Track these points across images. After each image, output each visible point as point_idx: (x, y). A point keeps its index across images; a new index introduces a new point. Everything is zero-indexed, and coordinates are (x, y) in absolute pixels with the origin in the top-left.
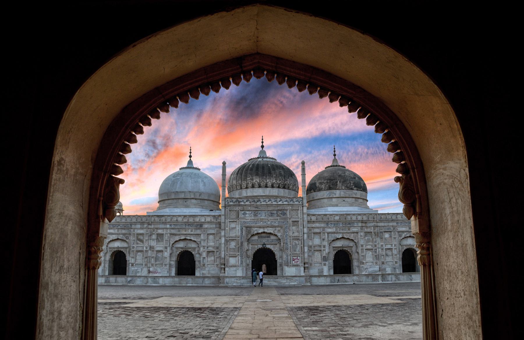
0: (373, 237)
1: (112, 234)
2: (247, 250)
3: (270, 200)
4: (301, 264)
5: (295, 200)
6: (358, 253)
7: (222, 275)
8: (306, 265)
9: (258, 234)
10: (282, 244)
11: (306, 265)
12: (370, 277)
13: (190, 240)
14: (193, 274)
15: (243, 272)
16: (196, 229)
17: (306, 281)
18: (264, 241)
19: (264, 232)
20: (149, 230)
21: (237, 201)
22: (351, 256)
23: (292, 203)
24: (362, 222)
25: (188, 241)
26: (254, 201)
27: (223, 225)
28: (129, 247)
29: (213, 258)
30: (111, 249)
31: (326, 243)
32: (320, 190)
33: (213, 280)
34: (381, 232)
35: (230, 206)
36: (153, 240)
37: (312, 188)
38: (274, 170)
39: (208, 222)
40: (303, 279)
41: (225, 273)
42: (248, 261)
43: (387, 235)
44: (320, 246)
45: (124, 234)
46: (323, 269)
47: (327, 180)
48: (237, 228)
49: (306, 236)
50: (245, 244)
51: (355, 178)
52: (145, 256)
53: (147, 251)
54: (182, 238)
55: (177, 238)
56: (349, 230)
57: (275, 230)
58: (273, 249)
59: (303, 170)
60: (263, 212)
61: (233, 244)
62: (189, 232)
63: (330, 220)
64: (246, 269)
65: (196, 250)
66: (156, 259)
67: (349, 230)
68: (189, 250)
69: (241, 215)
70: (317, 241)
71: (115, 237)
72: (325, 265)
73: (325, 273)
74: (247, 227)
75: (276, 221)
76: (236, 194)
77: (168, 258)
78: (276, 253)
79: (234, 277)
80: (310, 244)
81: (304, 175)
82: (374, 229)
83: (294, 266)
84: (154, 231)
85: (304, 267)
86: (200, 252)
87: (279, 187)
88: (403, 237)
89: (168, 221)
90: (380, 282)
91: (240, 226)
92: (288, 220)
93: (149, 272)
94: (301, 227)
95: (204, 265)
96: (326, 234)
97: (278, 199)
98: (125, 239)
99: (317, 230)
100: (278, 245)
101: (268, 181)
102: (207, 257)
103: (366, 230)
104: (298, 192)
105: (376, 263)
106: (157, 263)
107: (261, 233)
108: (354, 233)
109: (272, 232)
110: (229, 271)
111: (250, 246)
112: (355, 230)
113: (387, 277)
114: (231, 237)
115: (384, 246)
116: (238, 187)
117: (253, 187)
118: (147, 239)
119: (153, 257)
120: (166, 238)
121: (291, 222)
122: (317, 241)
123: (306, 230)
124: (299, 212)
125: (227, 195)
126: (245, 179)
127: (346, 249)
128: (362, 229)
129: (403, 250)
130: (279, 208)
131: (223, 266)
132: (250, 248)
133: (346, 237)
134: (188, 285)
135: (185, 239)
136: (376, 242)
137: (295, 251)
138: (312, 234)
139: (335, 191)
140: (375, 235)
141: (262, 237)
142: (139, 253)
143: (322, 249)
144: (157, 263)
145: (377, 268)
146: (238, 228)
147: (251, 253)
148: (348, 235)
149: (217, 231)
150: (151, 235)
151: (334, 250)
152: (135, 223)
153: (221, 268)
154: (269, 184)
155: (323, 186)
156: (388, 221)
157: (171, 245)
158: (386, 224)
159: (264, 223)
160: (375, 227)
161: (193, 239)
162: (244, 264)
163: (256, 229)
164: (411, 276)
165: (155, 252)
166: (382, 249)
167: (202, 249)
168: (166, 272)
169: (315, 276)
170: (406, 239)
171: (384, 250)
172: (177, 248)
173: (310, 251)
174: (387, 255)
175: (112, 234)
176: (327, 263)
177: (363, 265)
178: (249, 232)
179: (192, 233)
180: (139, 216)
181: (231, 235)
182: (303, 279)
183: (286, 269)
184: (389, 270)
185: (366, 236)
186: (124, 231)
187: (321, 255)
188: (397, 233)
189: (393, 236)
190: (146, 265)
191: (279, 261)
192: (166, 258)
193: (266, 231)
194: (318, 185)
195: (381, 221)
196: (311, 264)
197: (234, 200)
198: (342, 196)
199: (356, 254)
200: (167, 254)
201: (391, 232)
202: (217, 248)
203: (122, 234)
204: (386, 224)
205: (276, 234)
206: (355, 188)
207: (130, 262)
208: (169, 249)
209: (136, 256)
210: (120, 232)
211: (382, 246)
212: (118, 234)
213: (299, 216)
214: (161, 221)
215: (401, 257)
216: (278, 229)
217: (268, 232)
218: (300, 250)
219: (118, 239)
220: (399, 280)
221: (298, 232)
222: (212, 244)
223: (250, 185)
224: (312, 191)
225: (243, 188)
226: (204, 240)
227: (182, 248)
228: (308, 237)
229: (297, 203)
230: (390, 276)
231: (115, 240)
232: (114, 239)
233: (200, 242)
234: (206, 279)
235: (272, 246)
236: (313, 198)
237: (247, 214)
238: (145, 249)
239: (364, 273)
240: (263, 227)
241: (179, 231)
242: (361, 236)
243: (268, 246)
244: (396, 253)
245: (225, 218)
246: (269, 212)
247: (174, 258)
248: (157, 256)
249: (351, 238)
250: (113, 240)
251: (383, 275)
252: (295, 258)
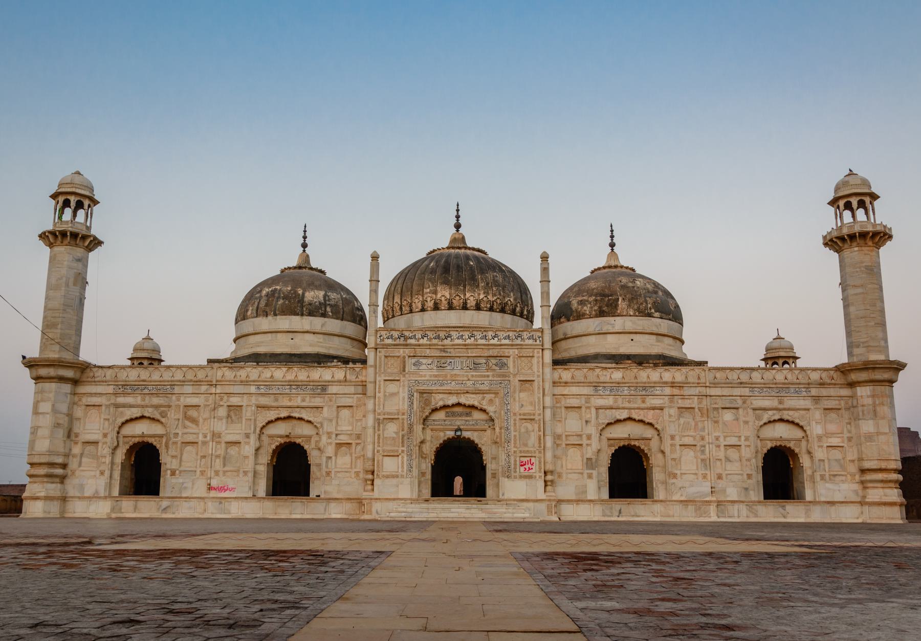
0: (698, 418)
1: (131, 406)
2: (422, 442)
3: (472, 336)
4: (538, 475)
5: (525, 335)
6: (663, 452)
7: (366, 495)
8: (549, 477)
9: (445, 407)
10: (497, 429)
11: (549, 477)
12: (691, 508)
13: (300, 419)
14: (307, 493)
15: (412, 491)
16: (314, 395)
17: (549, 512)
18: (459, 422)
19: (459, 404)
20: (211, 398)
21: (402, 336)
22: (648, 459)
23: (519, 341)
24: (673, 385)
25: (295, 422)
26: (438, 337)
27: (370, 387)
28: (166, 435)
29: (347, 459)
30: (126, 439)
31: (592, 430)
32: (580, 316)
33: (348, 506)
34: (716, 409)
35: (387, 346)
36: (220, 419)
37: (562, 313)
38: (482, 272)
39: (340, 381)
40: (543, 507)
41: (373, 490)
42: (424, 466)
43: (728, 416)
44: (580, 436)
45: (156, 407)
46: (586, 486)
47: (596, 295)
48: (401, 395)
49: (548, 413)
50: (418, 428)
51: (656, 293)
52: (200, 454)
53: (205, 443)
54: (282, 415)
55: (272, 415)
56: (643, 402)
57: (483, 398)
58: (476, 442)
59: (545, 270)
60: (457, 360)
61: (391, 429)
62: (298, 401)
63: (602, 379)
64: (420, 483)
65: (313, 441)
66: (225, 460)
67: (643, 402)
68: (298, 441)
69: (410, 367)
70: (573, 424)
71: (136, 412)
72: (590, 476)
73: (592, 494)
74: (422, 393)
75: (485, 378)
76: (400, 322)
77: (252, 458)
78: (483, 449)
79: (394, 499)
80: (559, 431)
81: (545, 280)
82: (700, 403)
83: (521, 477)
84: (222, 399)
85: (545, 481)
86: (321, 445)
87: (491, 309)
88: (765, 420)
89: (252, 378)
90: (714, 518)
91: (406, 389)
92: (511, 379)
93: (210, 488)
94: (538, 394)
95: (328, 474)
96: (593, 411)
97: (490, 334)
98: (158, 416)
99: (574, 402)
100: (489, 432)
101: (468, 295)
102: (336, 456)
103: (681, 403)
104: (532, 322)
105: (705, 476)
106: (226, 469)
107: (453, 406)
108: (654, 409)
109: (476, 404)
110: (382, 487)
111: (429, 433)
112: (657, 402)
113: (730, 507)
114: (389, 414)
115: (722, 439)
116: (406, 309)
117: (436, 307)
118: (206, 415)
119: (218, 456)
120: (249, 414)
121: (517, 384)
122: (573, 424)
123: (548, 401)
124: (535, 360)
125: (380, 324)
126: (421, 292)
127: (637, 443)
128: (671, 401)
129: (765, 451)
130: (491, 353)
131: (371, 476)
132: (428, 438)
133: (637, 418)
134: (294, 516)
135: (289, 418)
136: (703, 429)
137: (526, 445)
138: (563, 409)
139: (611, 319)
140: (702, 416)
141: (453, 414)
142: (189, 448)
143: (585, 441)
144: (226, 469)
145: (706, 488)
146: (404, 394)
147: (430, 449)
148: (642, 412)
149: (359, 400)
150: (214, 409)
151: (610, 446)
152: (183, 383)
153: (366, 480)
154: (472, 302)
155: (587, 309)
156: (729, 384)
157: (258, 429)
158: (726, 392)
159: (458, 380)
160: (701, 396)
161: (306, 418)
162: (415, 472)
163: (441, 396)
164: (783, 507)
165: (223, 445)
166: (719, 446)
167: (324, 439)
168: (247, 489)
169: (569, 501)
170: (771, 425)
171: (722, 448)
172: (270, 436)
173: (558, 445)
174: (728, 459)
175: (131, 406)
176: (595, 473)
177: (674, 481)
178: (427, 402)
179: (304, 404)
180: (190, 367)
181: (387, 409)
182: (543, 507)
183: (506, 483)
184: (732, 493)
185: (680, 416)
186: (156, 401)
187: (582, 456)
188: (750, 411)
189: (742, 419)
190: (202, 473)
191: (490, 467)
192: (246, 457)
193: (463, 400)
194: (575, 304)
195: (715, 385)
196: (560, 476)
197: (396, 334)
198: (627, 329)
199: (660, 455)
200: (248, 449)
201: (737, 408)
202: (358, 437)
203: (152, 406)
204: (726, 392)
205: (485, 407)
206: (657, 314)
207: (168, 466)
208: (253, 440)
209: (182, 454)
210: (148, 401)
211: (717, 439)
212: (143, 407)
213: (535, 370)
214: (238, 379)
215: (761, 465)
216: (488, 397)
217: (467, 403)
218: (537, 445)
219: (143, 417)
220: (756, 516)
221: (531, 403)
222: (345, 427)
223: (430, 304)
224: (562, 320)
225: (414, 309)
226: (331, 420)
227: (281, 437)
228: (554, 415)
229: (531, 342)
230: (736, 506)
231: (136, 419)
232: (134, 416)
233: (322, 424)
234: (333, 505)
235: (476, 434)
236: (565, 334)
237: (421, 364)
238: (201, 438)
239: (674, 498)
240: (457, 393)
241: (277, 400)
242: (670, 416)
243: (466, 434)
244: (748, 456)
245: (376, 373)
246: (471, 360)
247: (265, 458)
248: (226, 453)
249: (647, 421)
250: (132, 420)
251: (719, 503)
252: (525, 460)
